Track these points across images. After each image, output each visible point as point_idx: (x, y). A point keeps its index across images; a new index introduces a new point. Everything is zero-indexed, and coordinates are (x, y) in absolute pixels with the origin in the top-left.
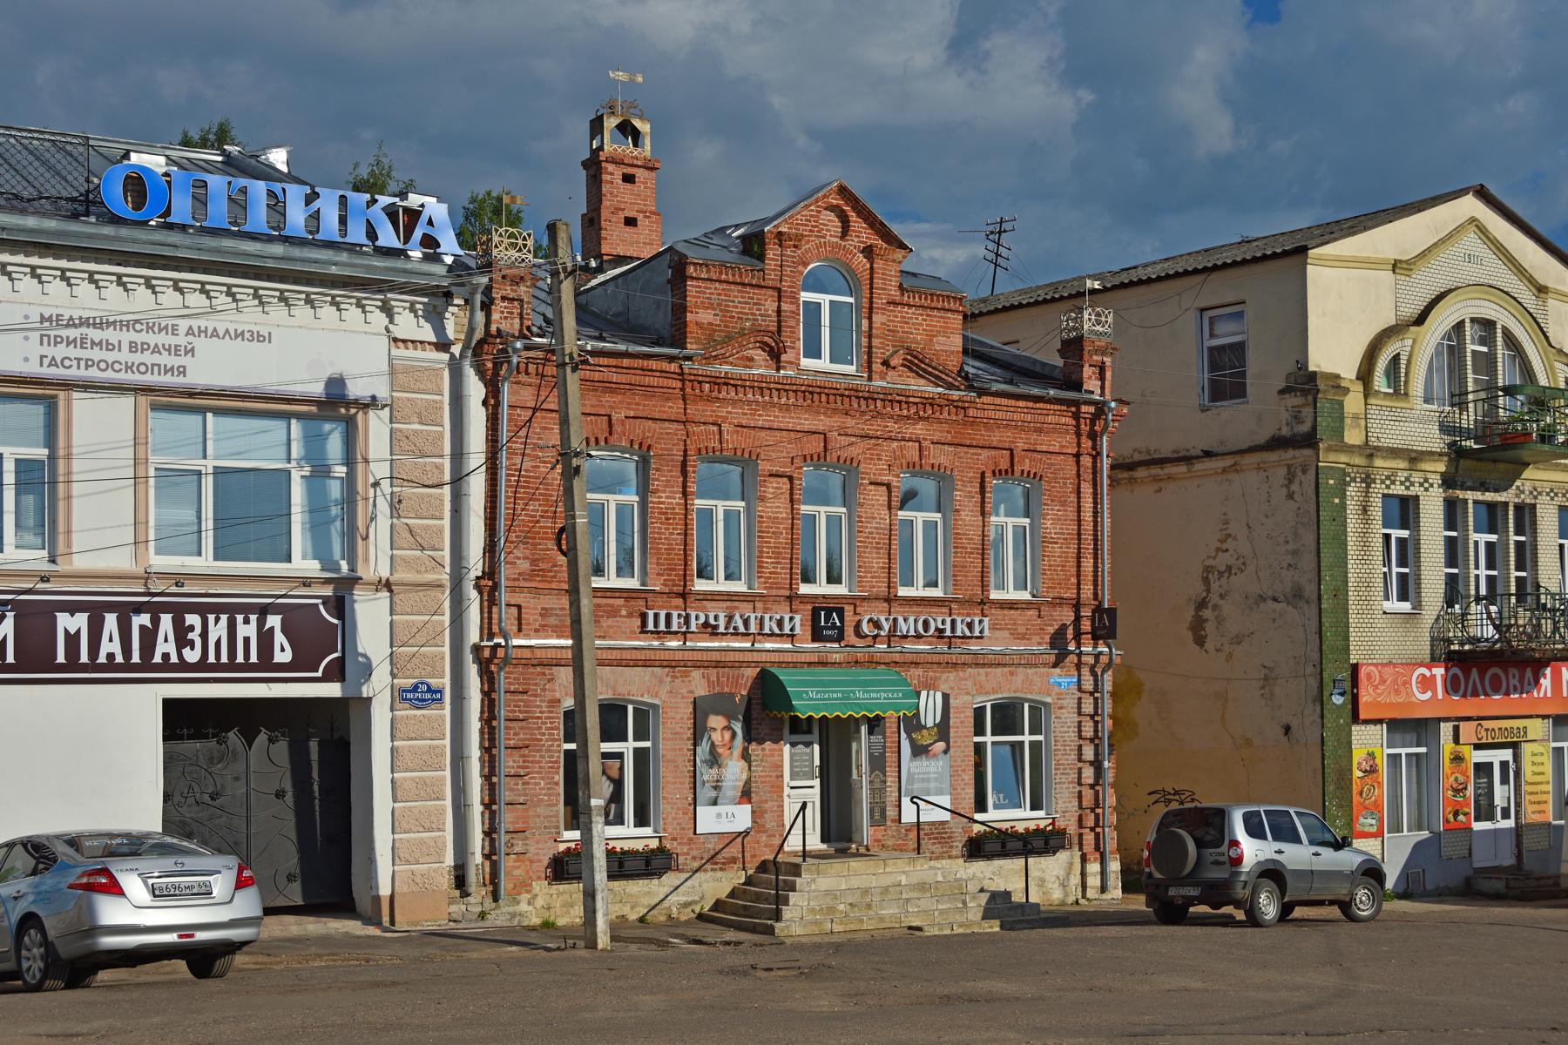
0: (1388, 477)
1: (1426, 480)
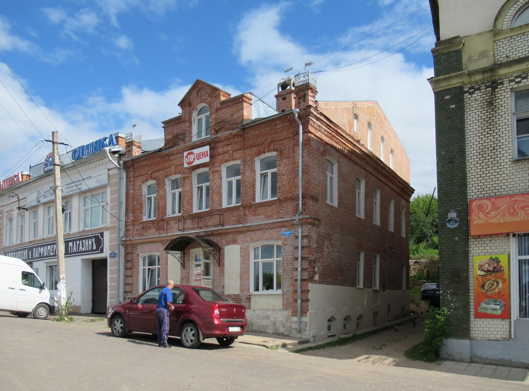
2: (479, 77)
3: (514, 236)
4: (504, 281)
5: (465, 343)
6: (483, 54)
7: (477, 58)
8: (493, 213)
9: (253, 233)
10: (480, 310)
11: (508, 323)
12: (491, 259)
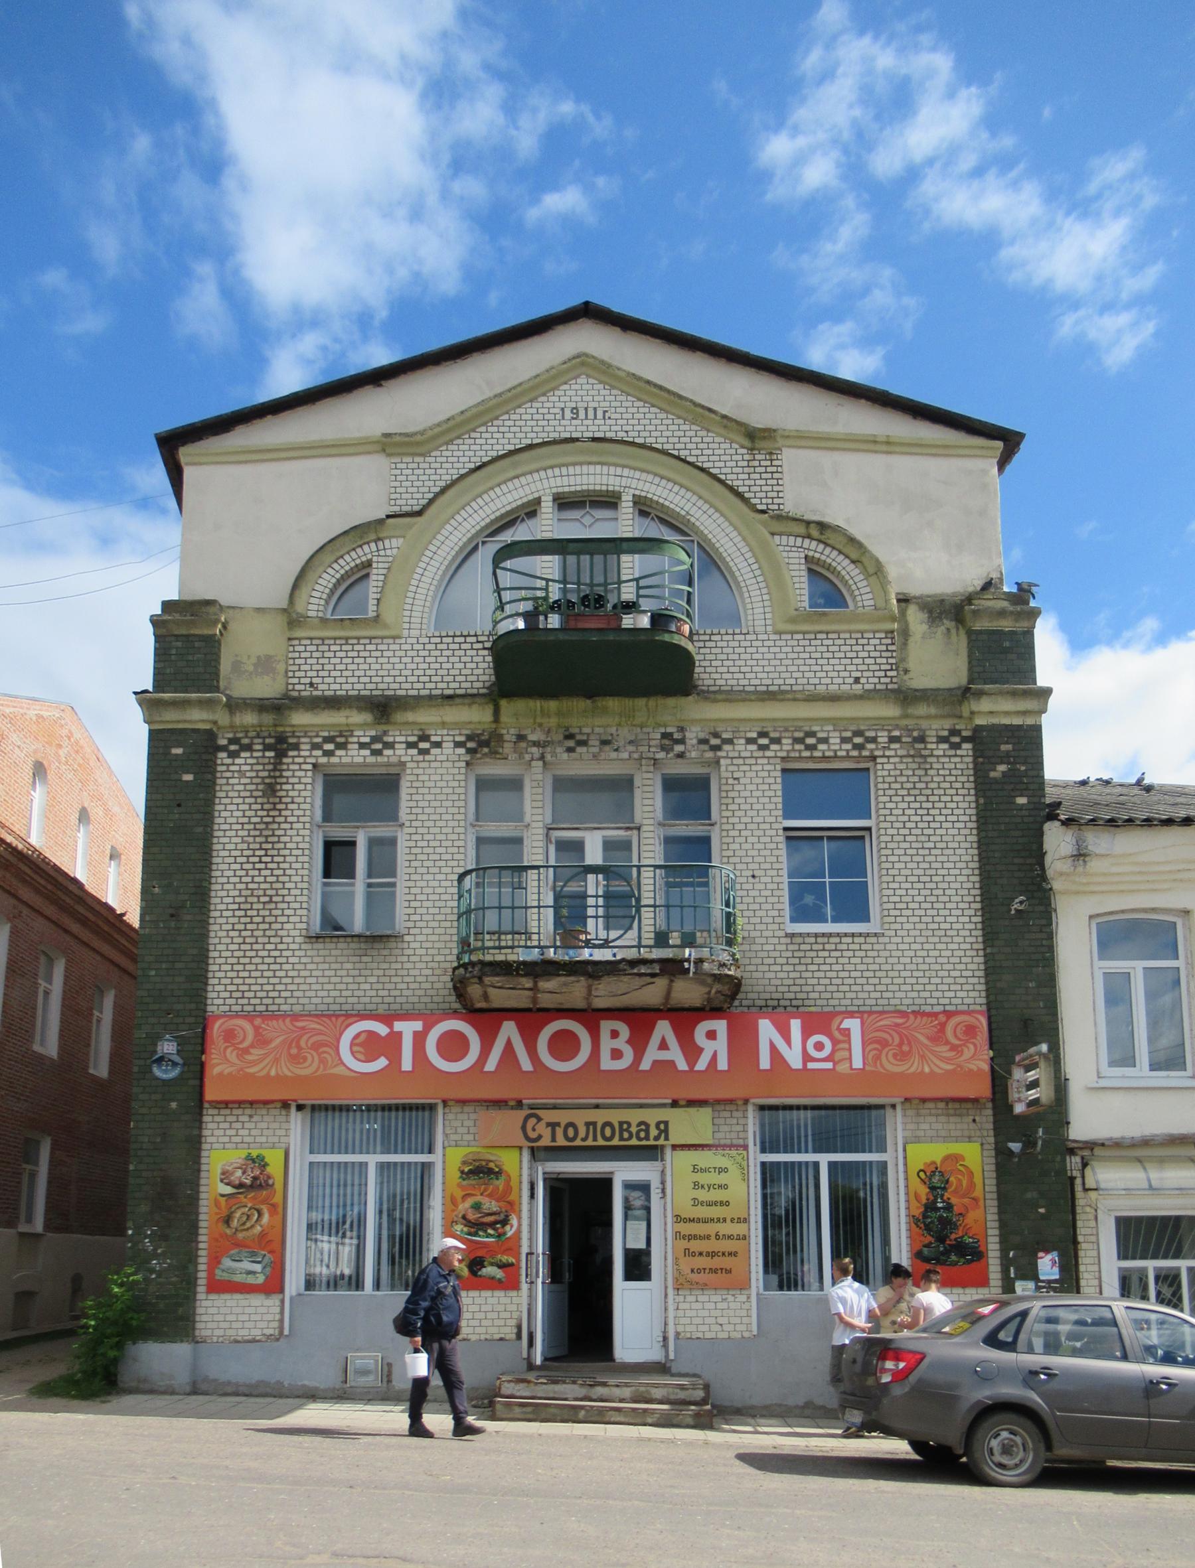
0: (328, 740)
2: (249, 718)
3: (300, 1108)
5: (181, 1349)
6: (265, 664)
7: (251, 668)
8: (256, 1053)
10: (219, 1275)
11: (278, 1303)
12: (249, 1158)
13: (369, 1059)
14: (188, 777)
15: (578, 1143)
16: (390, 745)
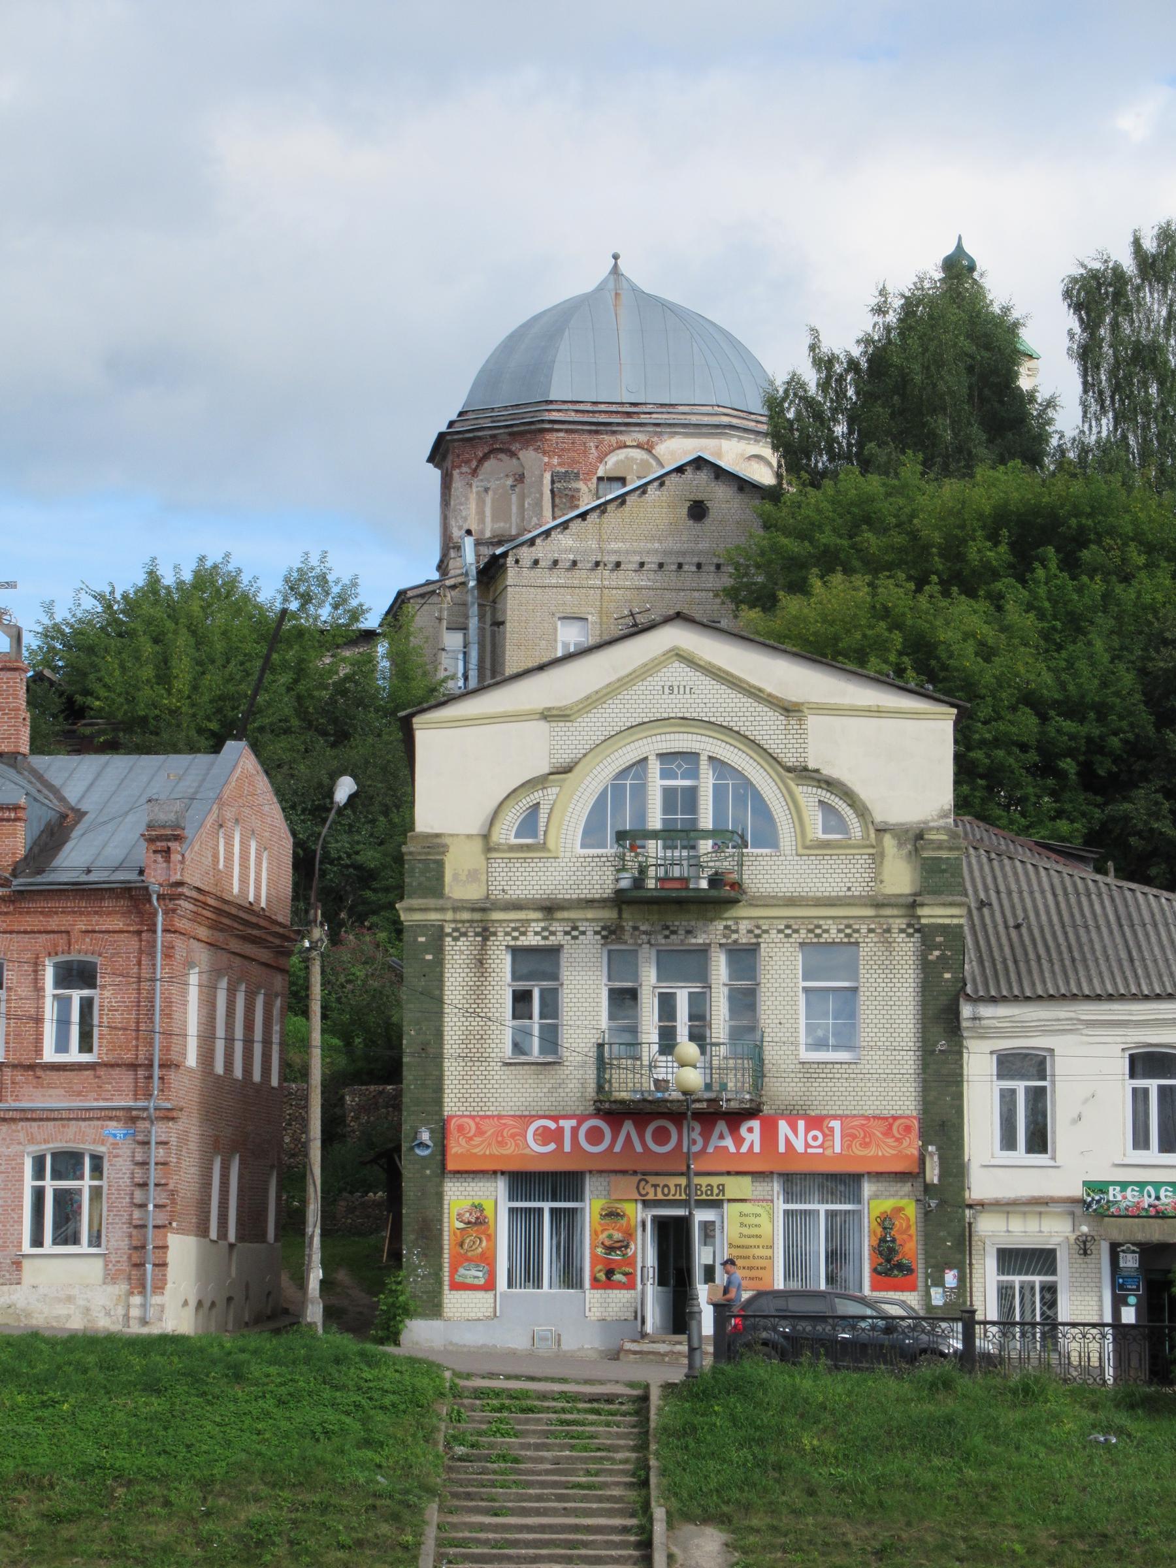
0: (515, 929)
1: (575, 928)
2: (466, 916)
3: (503, 1173)
4: (489, 1237)
5: (436, 1324)
6: (473, 875)
7: (464, 878)
8: (477, 1140)
9: (35, 1124)
10: (458, 1279)
12: (474, 1206)
13: (545, 1144)
14: (429, 957)
15: (670, 1197)
16: (553, 933)
